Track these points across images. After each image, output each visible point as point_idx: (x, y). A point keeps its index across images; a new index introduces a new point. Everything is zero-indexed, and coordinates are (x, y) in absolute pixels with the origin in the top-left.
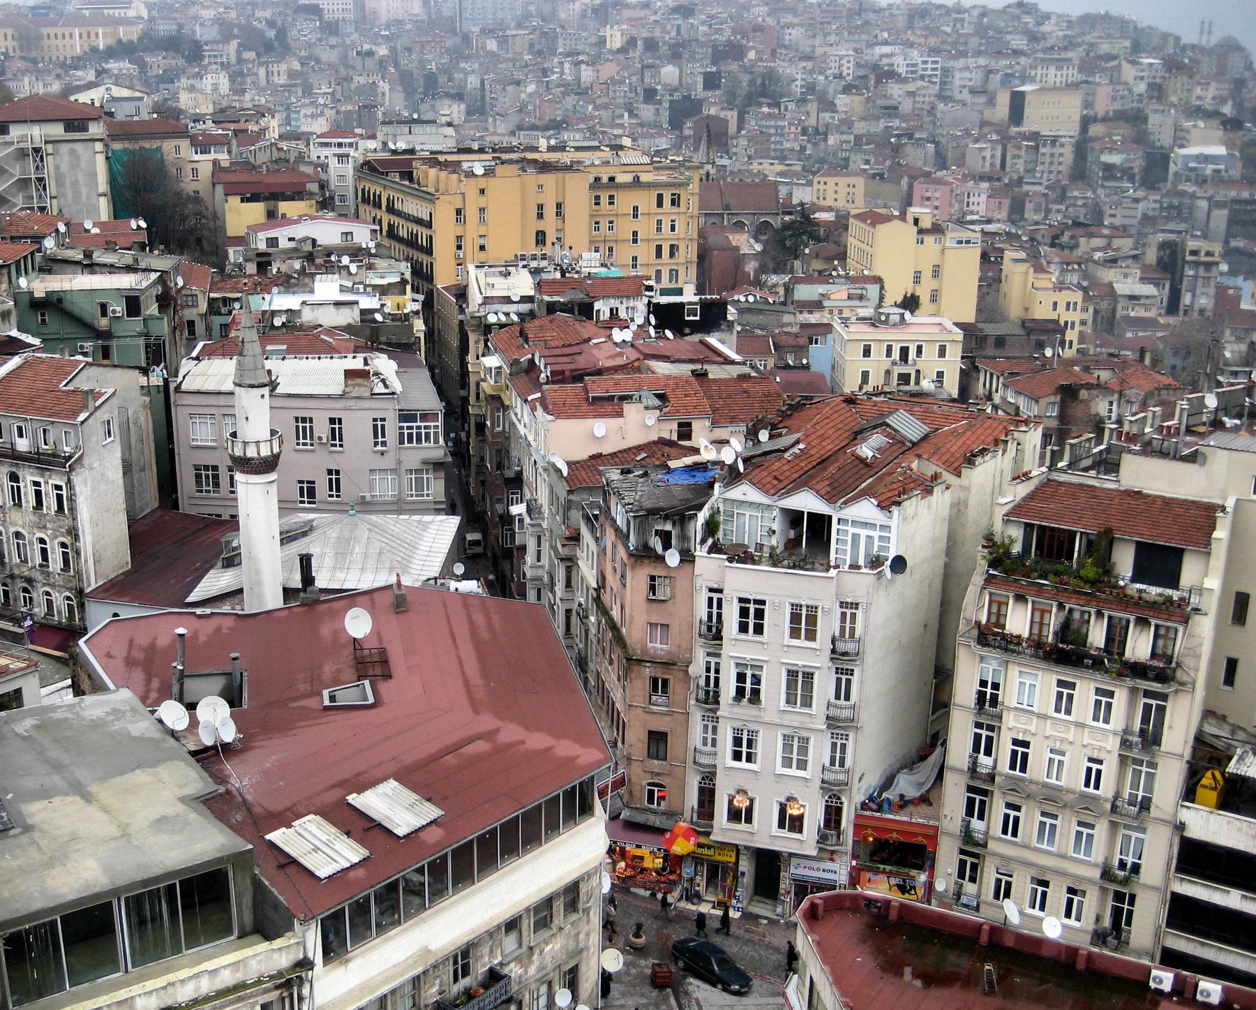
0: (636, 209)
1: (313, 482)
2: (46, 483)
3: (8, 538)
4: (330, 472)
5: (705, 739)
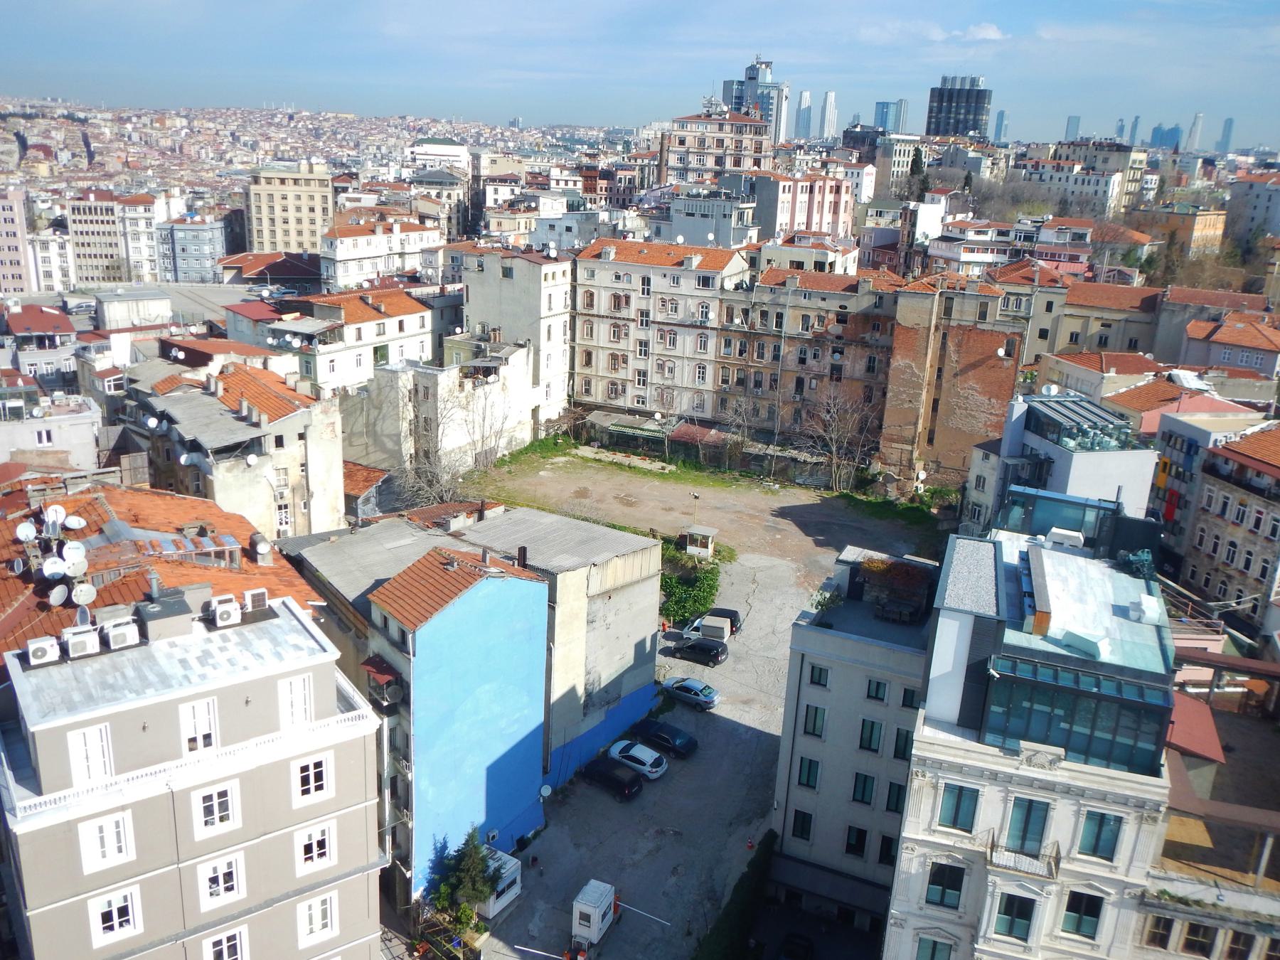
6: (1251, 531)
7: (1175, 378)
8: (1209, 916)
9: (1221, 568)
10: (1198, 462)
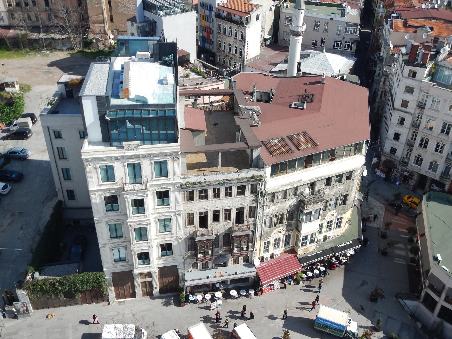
1: (317, 41)
2: (239, 30)
4: (322, 39)
5: (412, 138)
6: (234, 38)
8: (204, 186)
9: (228, 55)
10: (213, 13)
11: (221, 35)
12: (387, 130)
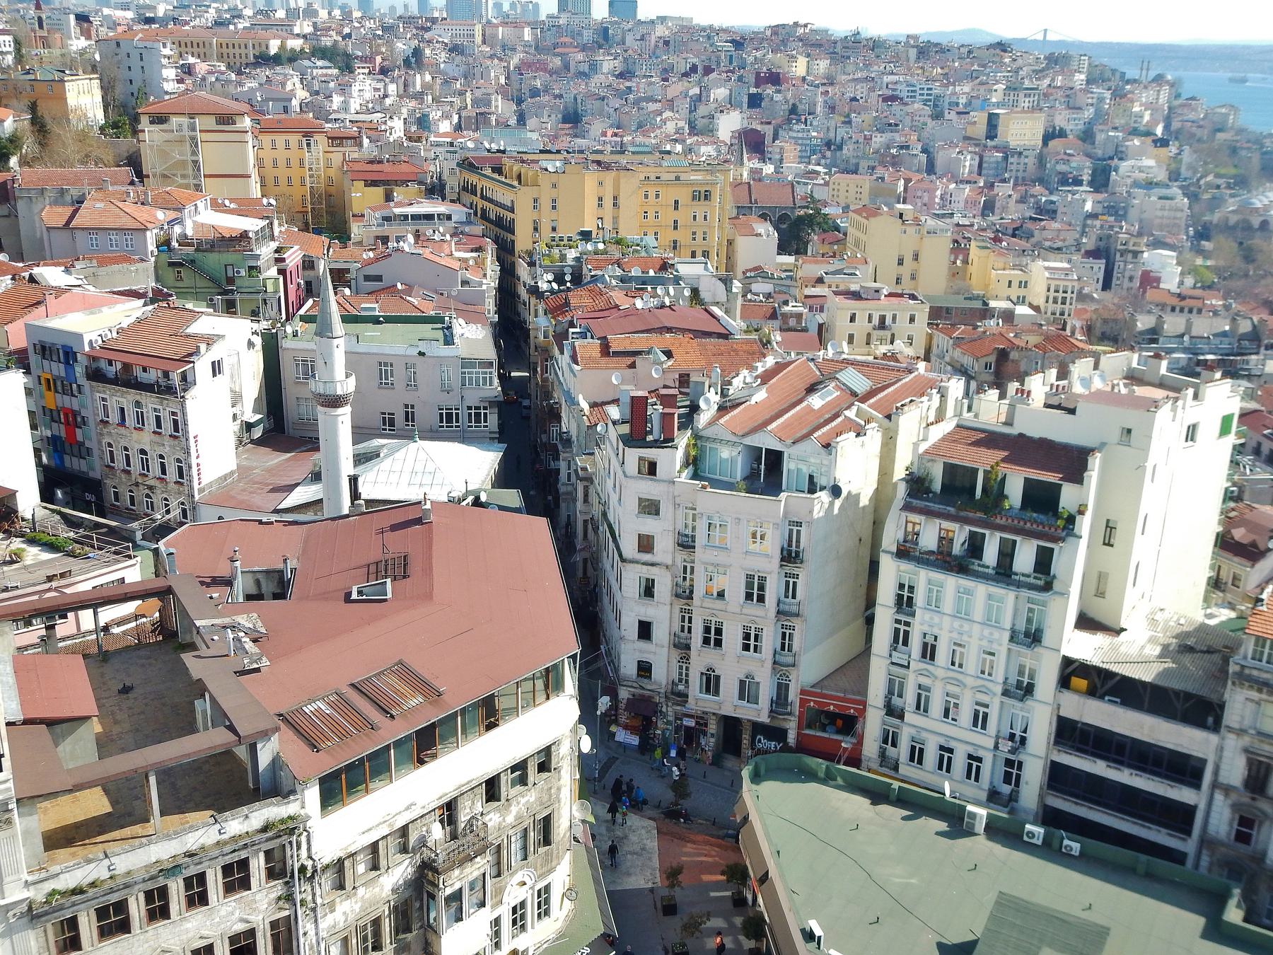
0: (676, 202)
1: (393, 414)
3: (134, 455)
5: (683, 627)
6: (154, 432)
7: (38, 278)
8: (112, 891)
10: (79, 370)
11: (111, 427)
12: (618, 618)
